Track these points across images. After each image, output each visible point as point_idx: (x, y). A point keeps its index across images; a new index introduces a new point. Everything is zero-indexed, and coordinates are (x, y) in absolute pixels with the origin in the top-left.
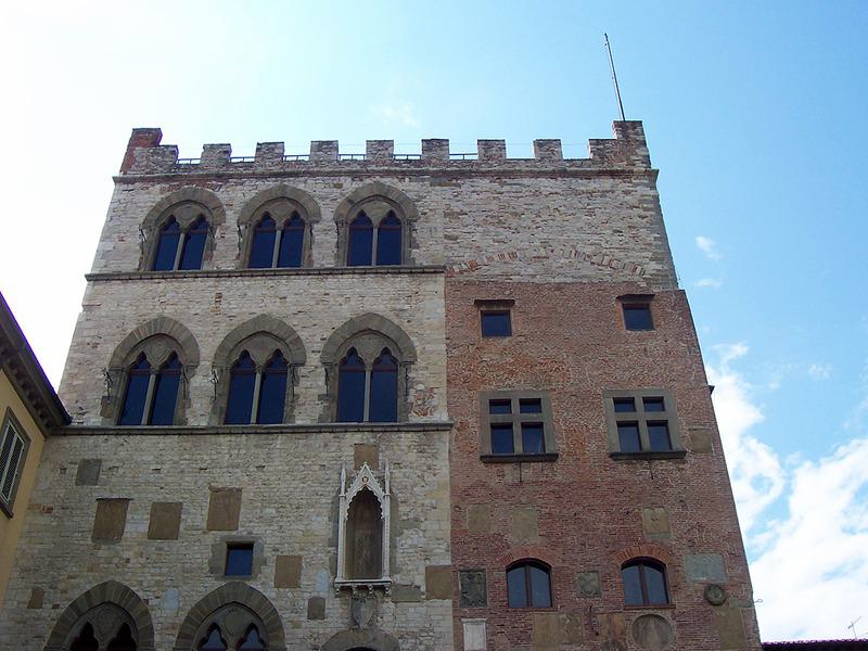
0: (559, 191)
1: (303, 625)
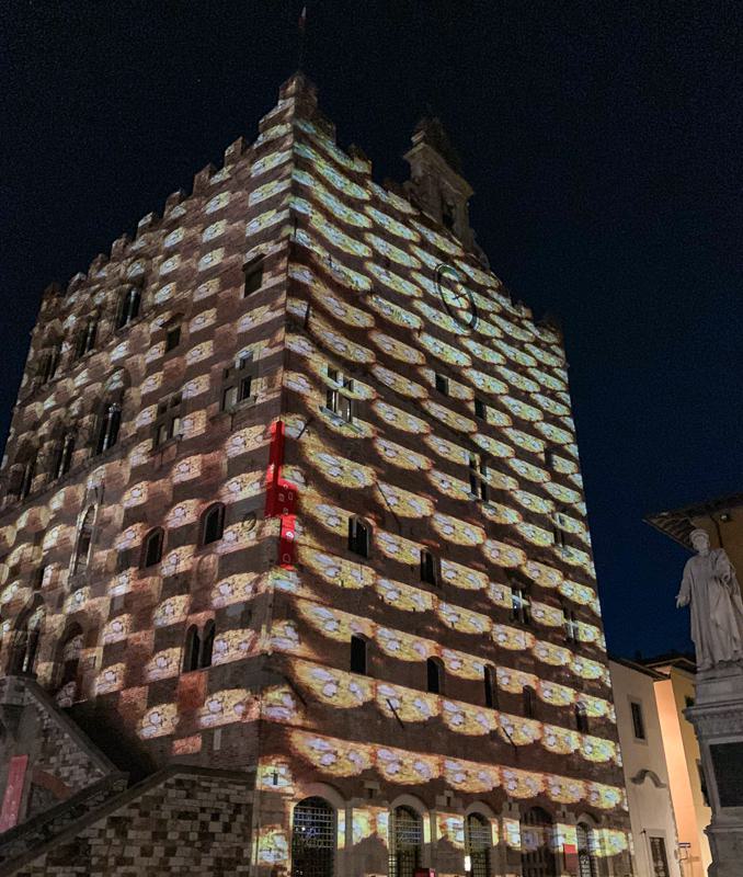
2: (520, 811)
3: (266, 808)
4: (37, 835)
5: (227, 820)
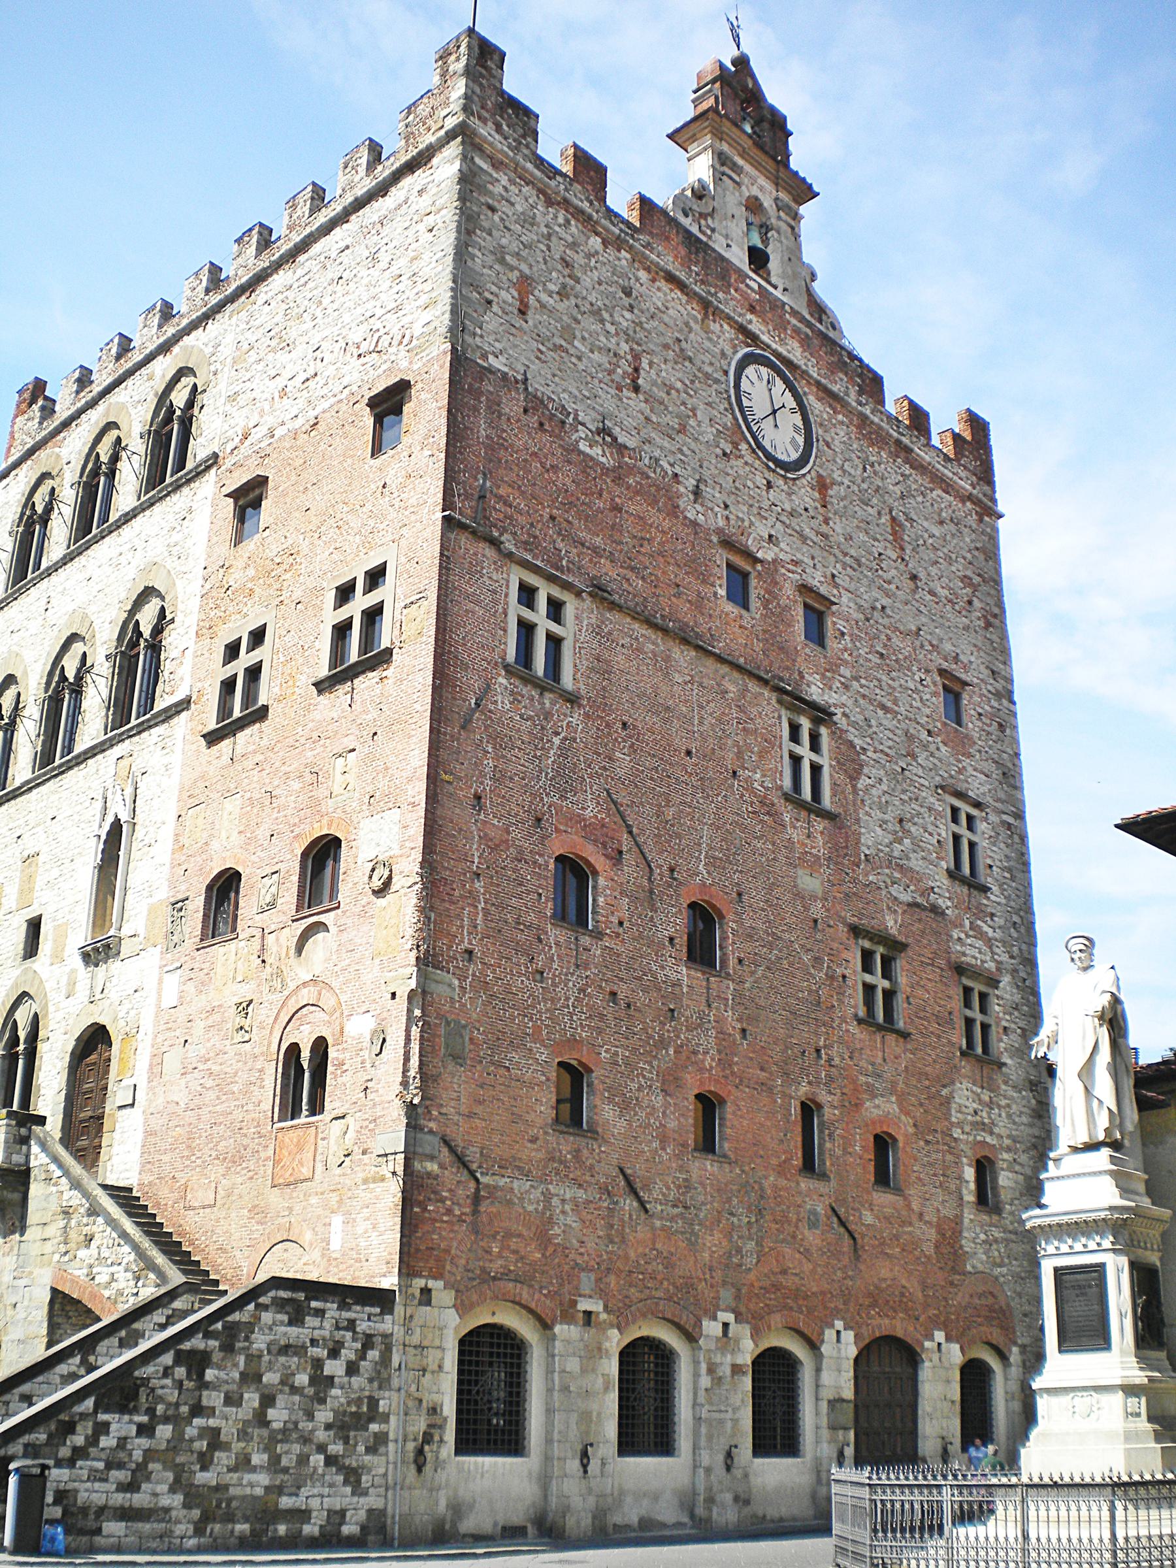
0: (348, 241)
2: (855, 1343)
3: (415, 1339)
4: (73, 1369)
5: (353, 1357)
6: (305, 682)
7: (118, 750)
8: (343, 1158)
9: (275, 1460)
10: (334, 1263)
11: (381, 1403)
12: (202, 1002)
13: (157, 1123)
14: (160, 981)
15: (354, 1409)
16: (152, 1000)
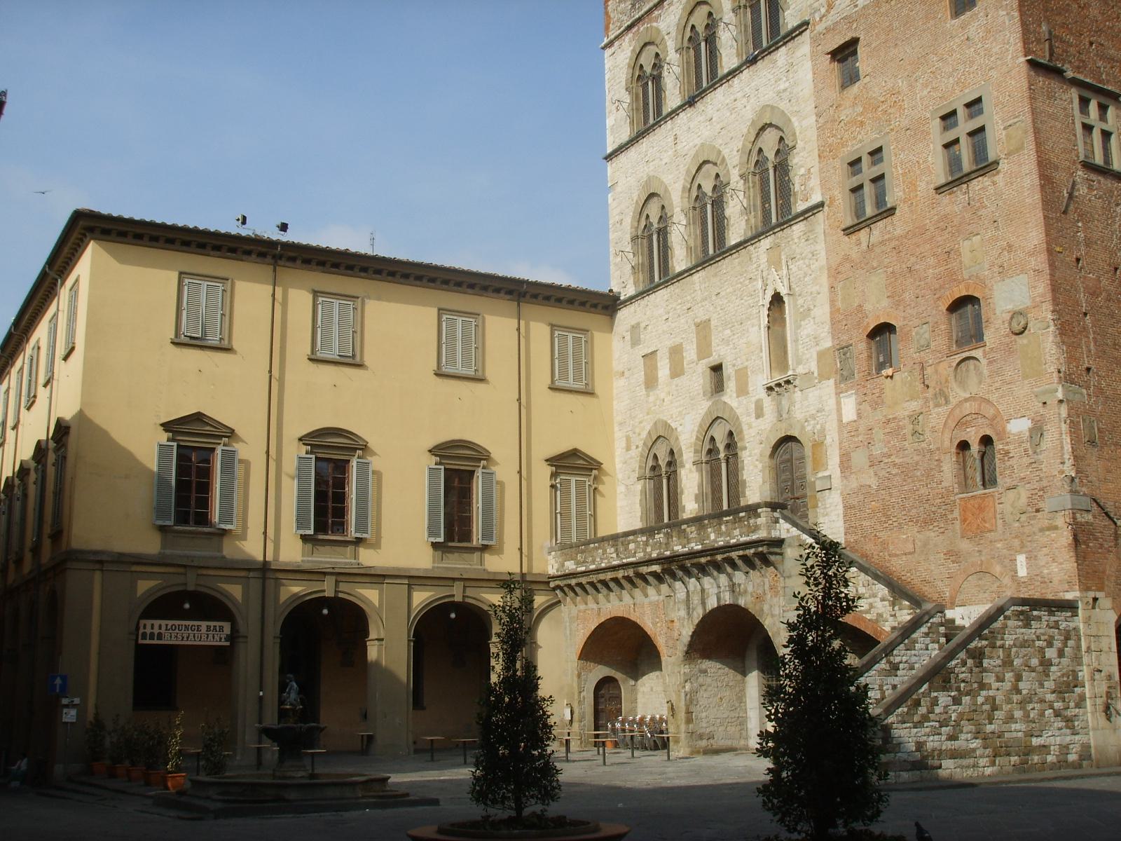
1: (754, 424)
6: (925, 187)
7: (766, 243)
8: (1019, 515)
9: (1027, 715)
10: (1023, 585)
11: (1080, 674)
12: (879, 415)
13: (854, 501)
14: (839, 403)
15: (1065, 679)
16: (834, 416)
